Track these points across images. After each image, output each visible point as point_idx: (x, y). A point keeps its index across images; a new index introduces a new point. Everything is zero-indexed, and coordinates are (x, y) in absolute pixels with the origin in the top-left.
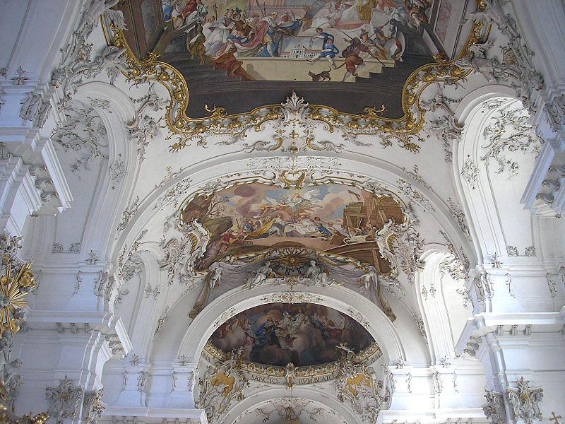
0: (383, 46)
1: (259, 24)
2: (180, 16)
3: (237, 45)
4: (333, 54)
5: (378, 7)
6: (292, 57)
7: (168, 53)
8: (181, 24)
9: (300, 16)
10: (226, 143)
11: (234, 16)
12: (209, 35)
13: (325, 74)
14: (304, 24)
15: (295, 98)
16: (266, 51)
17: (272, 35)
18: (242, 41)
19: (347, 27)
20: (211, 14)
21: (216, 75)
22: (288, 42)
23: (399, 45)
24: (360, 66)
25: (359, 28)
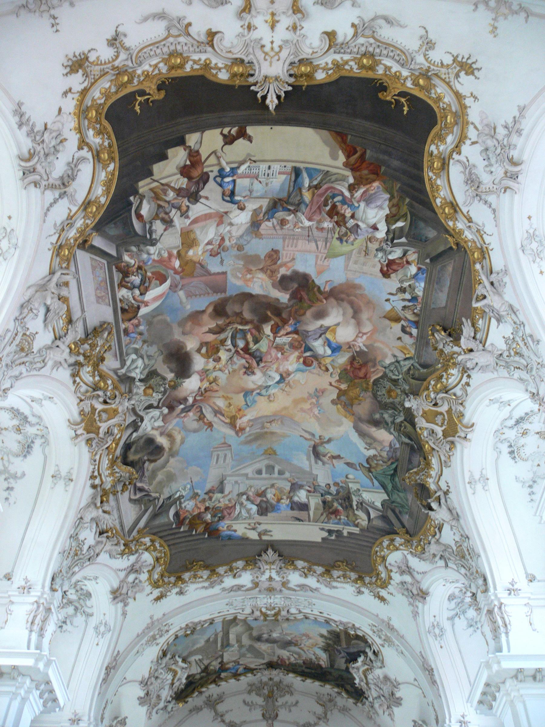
0: (159, 206)
1: (317, 217)
2: (408, 263)
3: (347, 194)
4: (222, 174)
5: (175, 252)
6: (276, 167)
7: (434, 228)
8: (409, 253)
9: (266, 226)
10: (388, 21)
11: (346, 234)
12: (379, 221)
13: (229, 140)
14: (262, 215)
15: (272, 102)
16: (310, 177)
17: (301, 202)
18: (339, 198)
19: (207, 217)
20: (374, 246)
21: (381, 156)
22: (282, 189)
23: (139, 217)
24: (182, 164)
25: (192, 219)
